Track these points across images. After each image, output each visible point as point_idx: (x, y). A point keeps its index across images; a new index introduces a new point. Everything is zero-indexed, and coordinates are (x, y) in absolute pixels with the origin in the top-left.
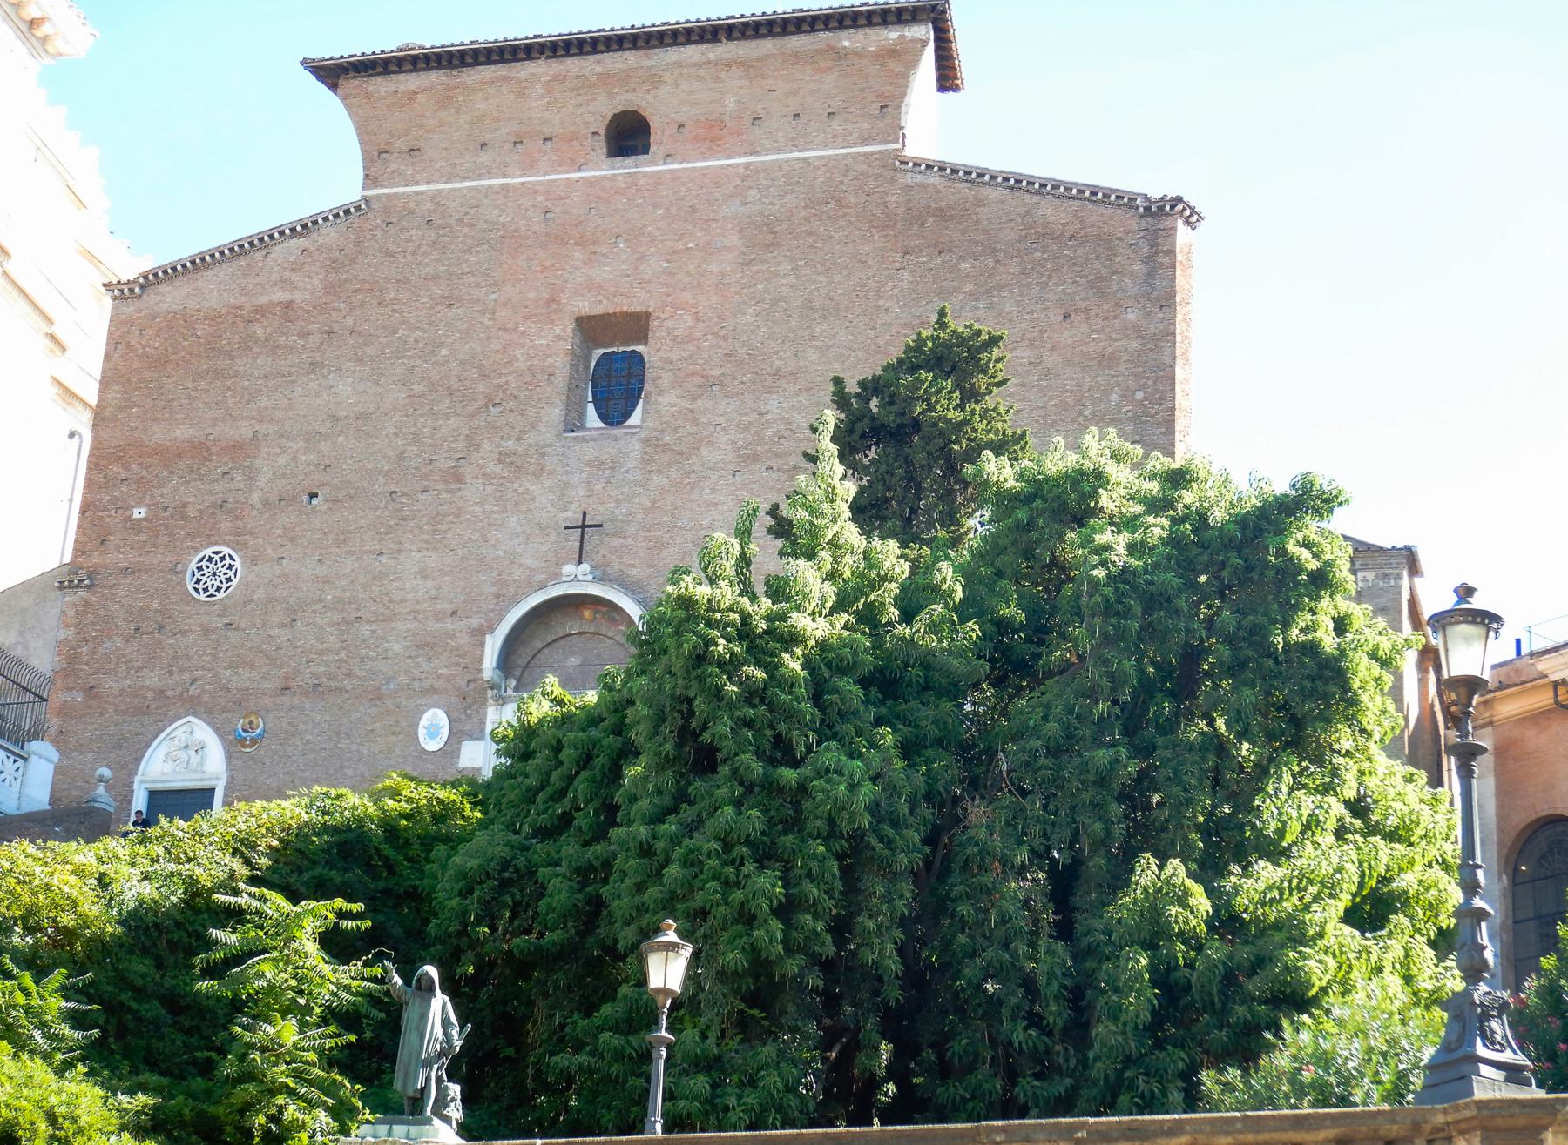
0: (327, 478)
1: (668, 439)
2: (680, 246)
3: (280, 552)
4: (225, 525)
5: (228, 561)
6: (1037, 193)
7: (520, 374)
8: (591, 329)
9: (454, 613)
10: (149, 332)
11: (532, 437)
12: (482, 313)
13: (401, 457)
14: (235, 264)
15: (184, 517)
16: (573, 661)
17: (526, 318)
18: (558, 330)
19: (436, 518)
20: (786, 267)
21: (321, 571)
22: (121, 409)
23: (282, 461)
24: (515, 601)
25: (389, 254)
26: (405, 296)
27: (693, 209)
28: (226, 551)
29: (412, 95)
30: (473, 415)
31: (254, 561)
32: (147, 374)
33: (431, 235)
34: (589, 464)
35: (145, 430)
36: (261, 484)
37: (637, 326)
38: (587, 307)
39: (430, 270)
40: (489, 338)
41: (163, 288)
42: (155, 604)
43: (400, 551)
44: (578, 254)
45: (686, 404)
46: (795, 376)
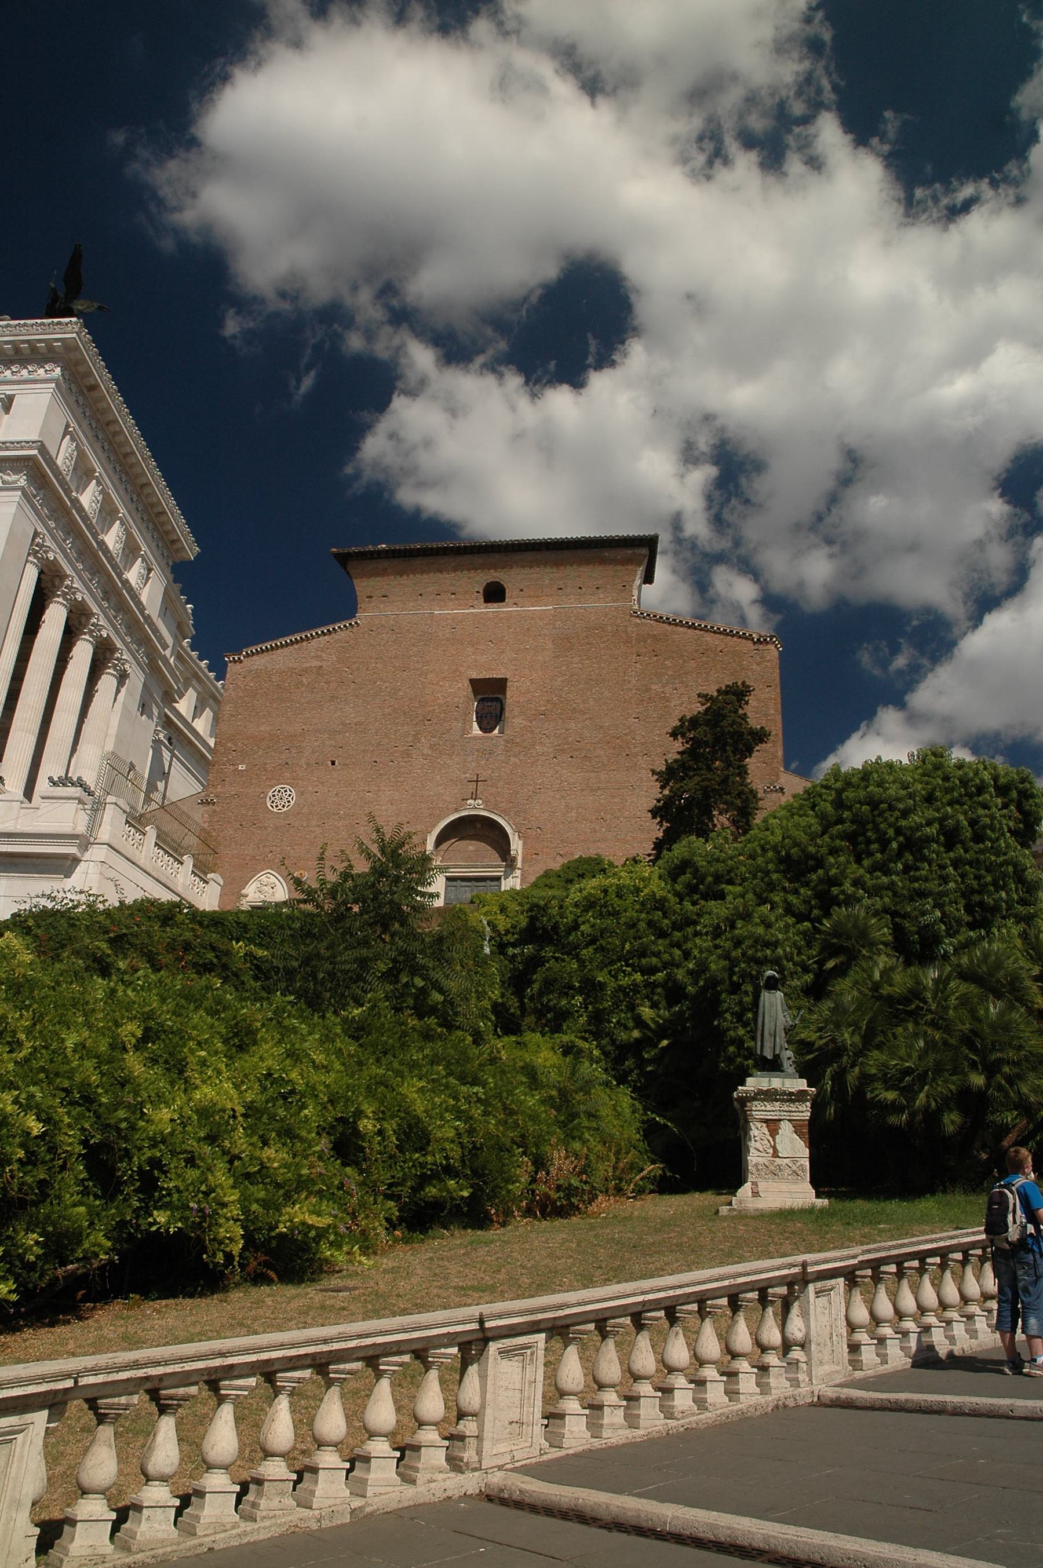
2: (522, 647)
3: (316, 789)
4: (287, 775)
5: (289, 792)
6: (701, 630)
7: (440, 706)
11: (446, 737)
12: (420, 675)
13: (379, 745)
14: (291, 648)
15: (265, 770)
16: (471, 848)
18: (460, 685)
20: (576, 659)
22: (232, 716)
24: (441, 818)
25: (372, 645)
27: (528, 629)
31: (302, 793)
34: (478, 751)
35: (245, 727)
37: (500, 685)
38: (475, 676)
40: (424, 688)
41: (255, 658)
42: (250, 813)
43: (379, 791)
44: (470, 649)
45: (525, 723)
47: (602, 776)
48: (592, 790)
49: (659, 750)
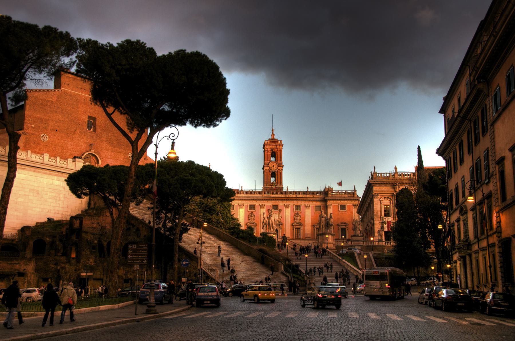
0: (59, 128)
1: (98, 135)
4: (45, 131)
7: (82, 121)
8: (89, 117)
9: (75, 151)
10: (33, 99)
11: (83, 130)
12: (77, 111)
14: (44, 92)
17: (82, 114)
19: (72, 138)
21: (59, 141)
23: (53, 124)
26: (67, 105)
28: (46, 135)
29: (70, 77)
30: (77, 125)
32: (33, 105)
33: (70, 98)
36: (50, 126)
38: (89, 114)
39: (70, 103)
41: (34, 92)
46: (112, 131)
47: (115, 148)
48: (113, 152)
49: (126, 145)
